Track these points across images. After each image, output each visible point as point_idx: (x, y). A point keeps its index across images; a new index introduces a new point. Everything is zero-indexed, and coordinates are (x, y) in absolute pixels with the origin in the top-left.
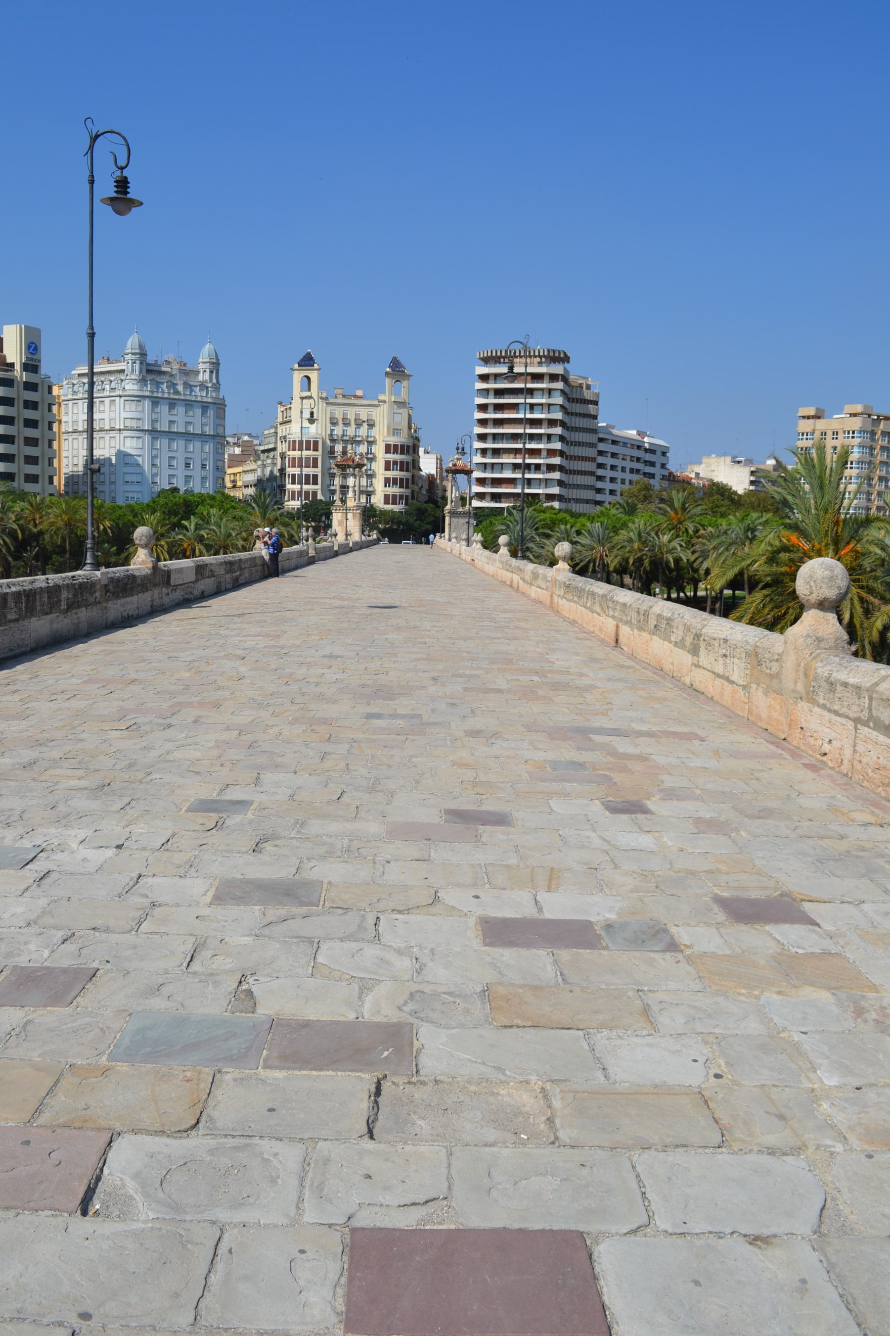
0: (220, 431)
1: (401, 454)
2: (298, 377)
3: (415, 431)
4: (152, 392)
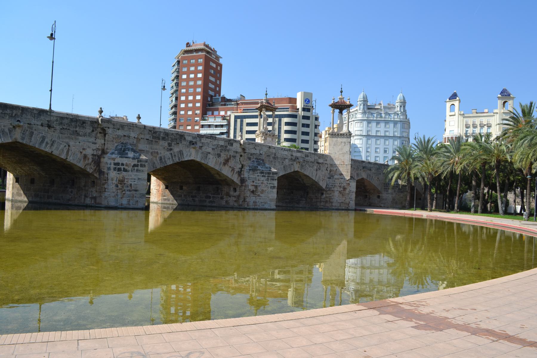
0: (405, 134)
2: (448, 105)
4: (368, 117)
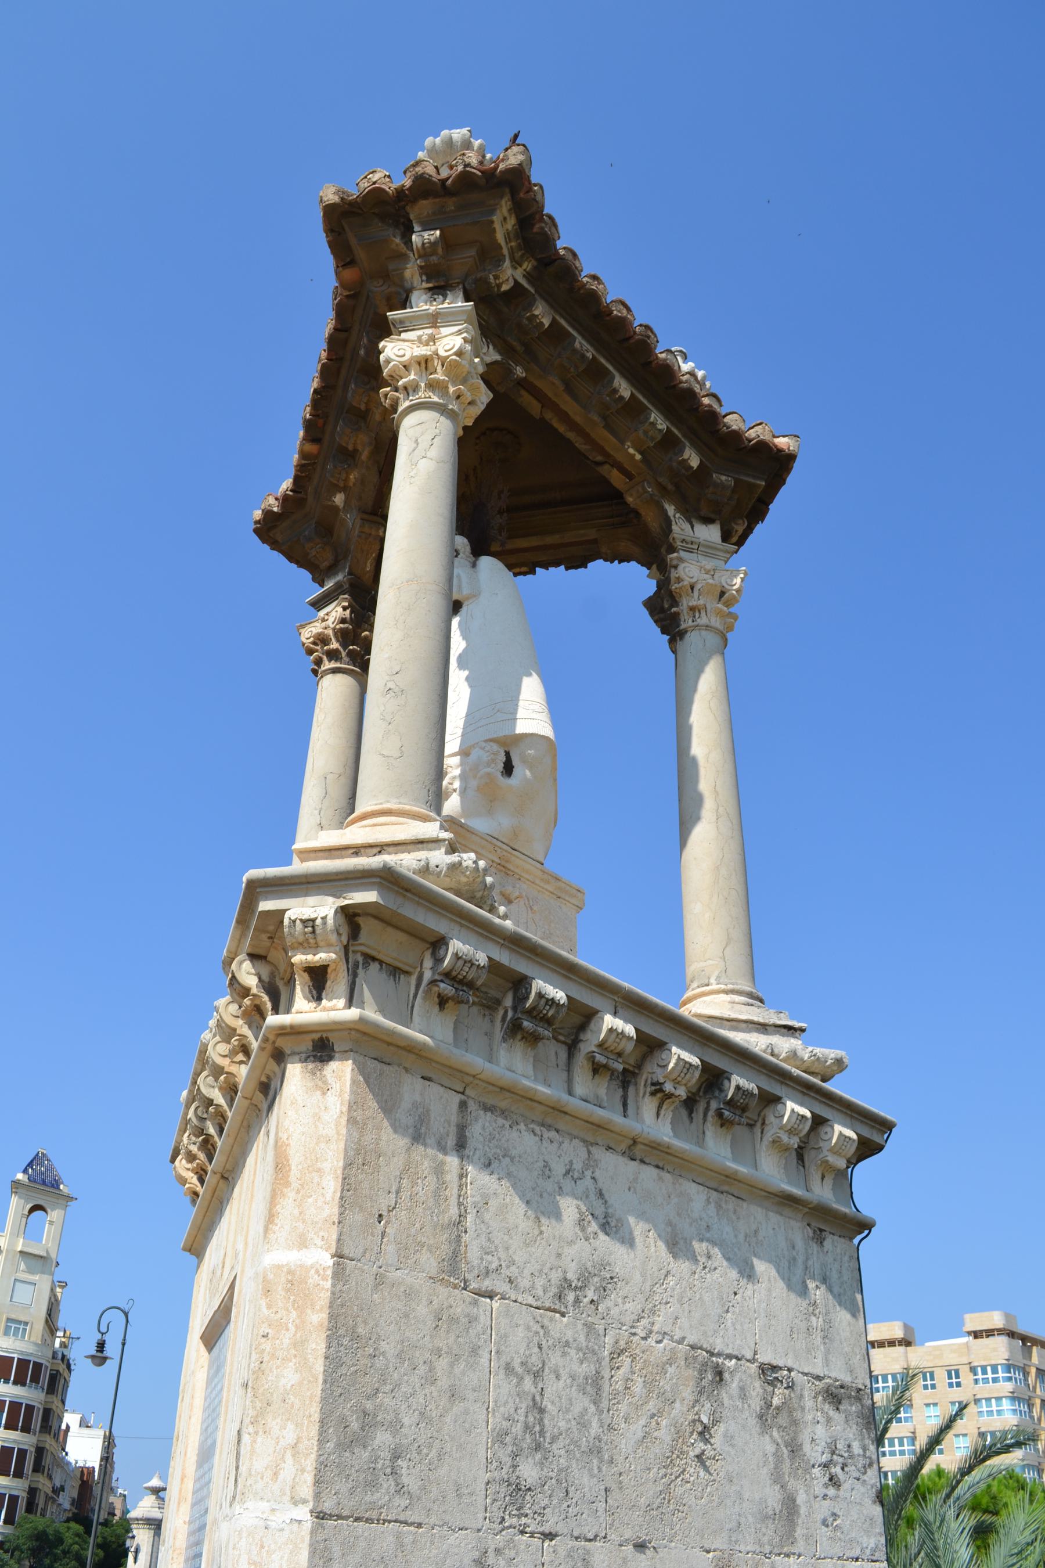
1: (15, 1383)
3: (63, 1345)
